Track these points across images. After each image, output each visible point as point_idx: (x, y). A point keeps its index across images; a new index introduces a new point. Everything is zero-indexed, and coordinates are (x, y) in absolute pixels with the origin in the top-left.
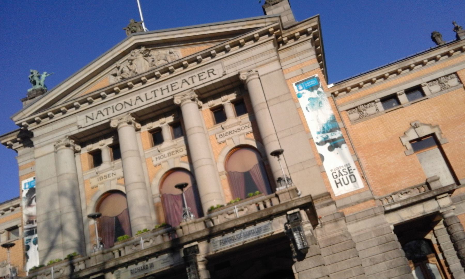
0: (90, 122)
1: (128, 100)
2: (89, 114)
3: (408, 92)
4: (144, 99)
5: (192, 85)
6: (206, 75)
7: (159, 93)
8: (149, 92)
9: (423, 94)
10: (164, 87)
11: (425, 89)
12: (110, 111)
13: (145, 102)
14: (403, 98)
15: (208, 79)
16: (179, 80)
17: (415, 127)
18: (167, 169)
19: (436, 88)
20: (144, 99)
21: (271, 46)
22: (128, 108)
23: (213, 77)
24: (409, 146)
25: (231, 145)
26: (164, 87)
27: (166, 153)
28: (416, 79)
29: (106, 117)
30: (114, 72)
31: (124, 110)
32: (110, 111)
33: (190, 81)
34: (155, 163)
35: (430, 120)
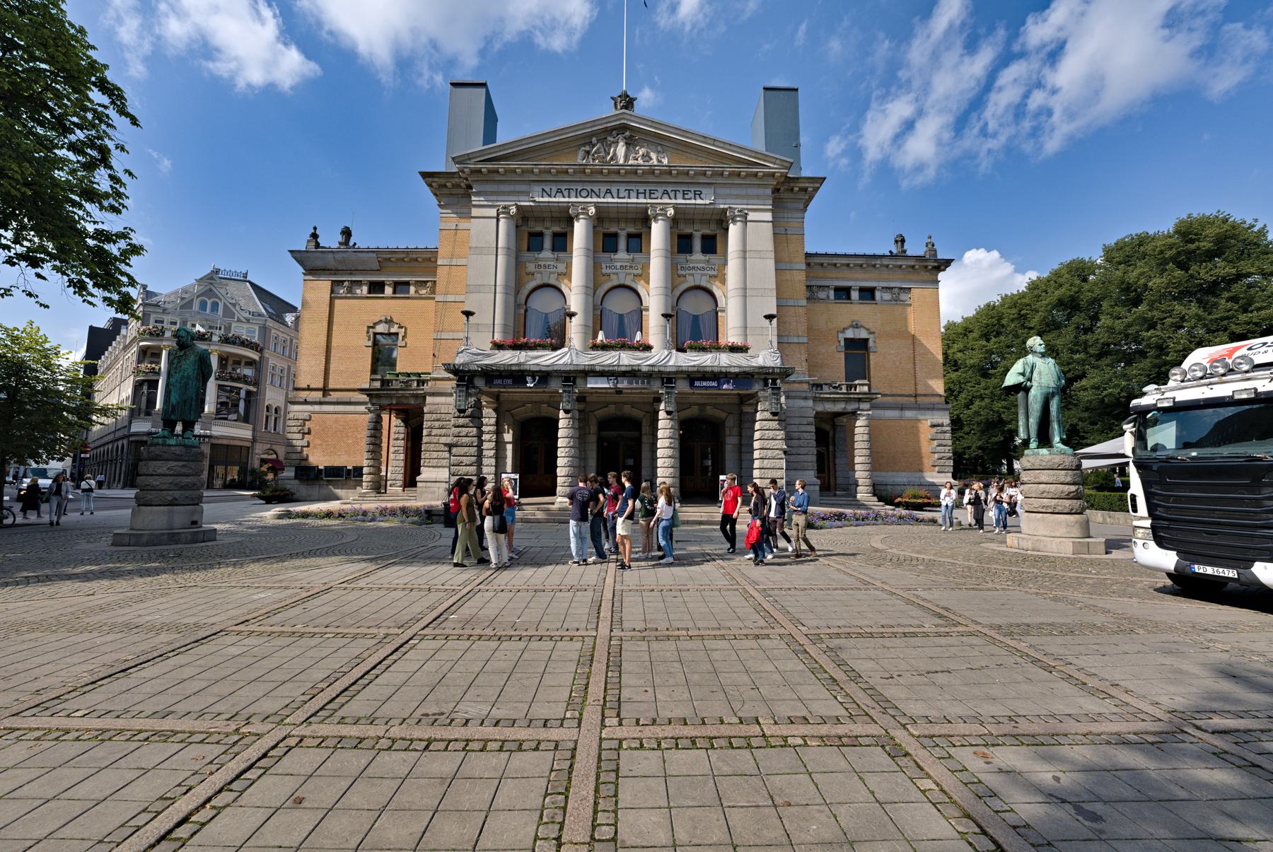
0: (546, 199)
1: (596, 190)
2: (547, 189)
3: (862, 290)
4: (615, 194)
5: (673, 201)
6: (692, 195)
7: (633, 194)
8: (622, 188)
9: (873, 298)
10: (641, 190)
11: (878, 294)
12: (573, 193)
13: (616, 200)
14: (855, 295)
15: (693, 201)
16: (661, 190)
17: (856, 326)
18: (615, 283)
19: (887, 296)
20: (615, 194)
21: (769, 191)
22: (595, 200)
23: (699, 201)
24: (842, 343)
25: (690, 282)
26: (641, 190)
27: (618, 265)
28: (875, 280)
29: (567, 200)
30: (587, 148)
31: (588, 200)
32: (573, 193)
33: (672, 195)
34: (604, 271)
35: (869, 326)
